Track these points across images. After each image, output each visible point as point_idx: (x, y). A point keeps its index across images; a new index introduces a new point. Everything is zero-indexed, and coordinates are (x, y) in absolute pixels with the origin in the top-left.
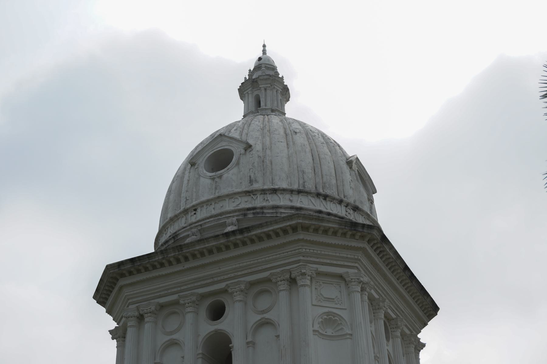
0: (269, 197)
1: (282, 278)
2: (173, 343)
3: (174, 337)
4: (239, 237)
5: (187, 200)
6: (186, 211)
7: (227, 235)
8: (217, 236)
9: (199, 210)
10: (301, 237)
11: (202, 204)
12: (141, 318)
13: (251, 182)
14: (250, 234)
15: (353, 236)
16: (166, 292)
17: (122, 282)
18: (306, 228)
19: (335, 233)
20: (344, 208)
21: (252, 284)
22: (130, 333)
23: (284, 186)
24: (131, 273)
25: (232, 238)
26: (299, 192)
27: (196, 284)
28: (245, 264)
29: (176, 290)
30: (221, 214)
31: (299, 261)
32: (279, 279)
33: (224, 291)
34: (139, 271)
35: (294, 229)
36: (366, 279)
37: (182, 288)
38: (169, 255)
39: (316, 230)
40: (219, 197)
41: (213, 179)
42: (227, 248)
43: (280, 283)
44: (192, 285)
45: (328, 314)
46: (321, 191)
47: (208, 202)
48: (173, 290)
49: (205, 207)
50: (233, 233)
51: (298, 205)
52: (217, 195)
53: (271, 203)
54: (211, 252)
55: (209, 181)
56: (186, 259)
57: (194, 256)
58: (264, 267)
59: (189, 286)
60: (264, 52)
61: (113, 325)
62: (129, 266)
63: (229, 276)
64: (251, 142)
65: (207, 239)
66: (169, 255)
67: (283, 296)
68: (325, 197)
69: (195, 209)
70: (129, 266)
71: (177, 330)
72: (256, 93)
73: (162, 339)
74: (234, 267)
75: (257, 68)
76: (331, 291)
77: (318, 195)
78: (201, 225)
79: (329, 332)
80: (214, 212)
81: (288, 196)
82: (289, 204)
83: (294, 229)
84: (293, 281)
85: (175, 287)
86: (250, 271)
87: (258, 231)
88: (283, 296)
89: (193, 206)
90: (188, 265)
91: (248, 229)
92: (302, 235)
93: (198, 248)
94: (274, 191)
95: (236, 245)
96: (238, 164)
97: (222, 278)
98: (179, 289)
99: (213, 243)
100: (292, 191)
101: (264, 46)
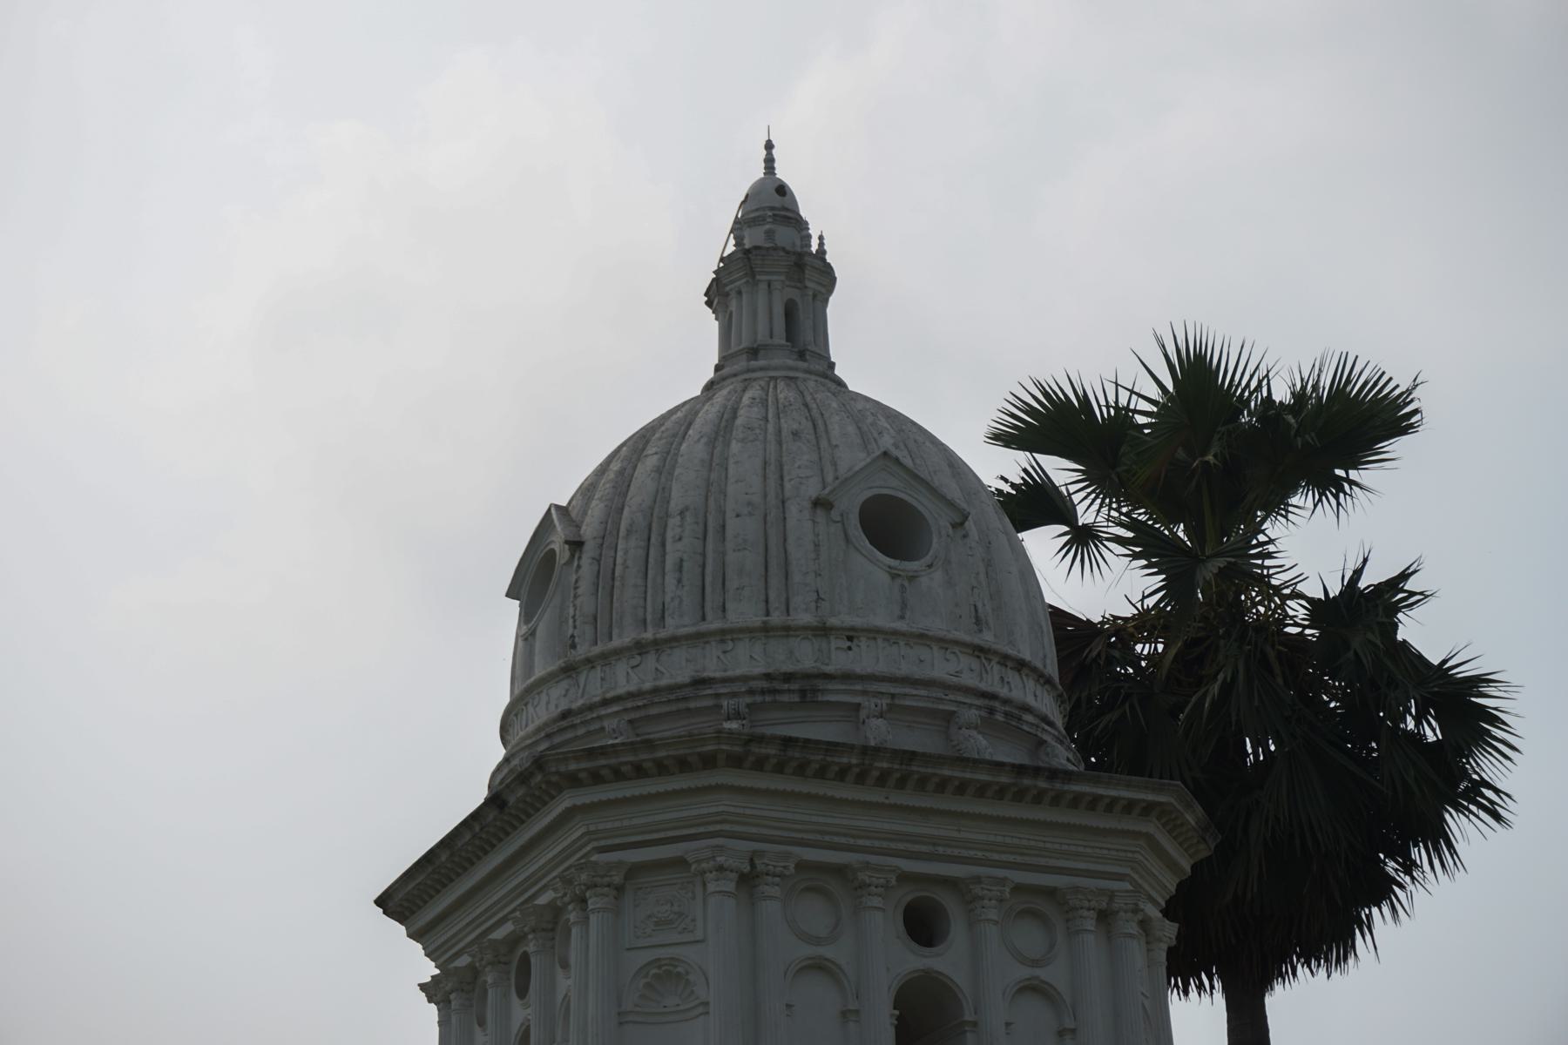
1: (1093, 904)
4: (1042, 784)
5: (819, 599)
6: (823, 631)
8: (1000, 765)
9: (863, 643)
11: (874, 633)
12: (748, 880)
13: (978, 621)
14: (1066, 787)
16: (819, 837)
24: (759, 765)
25: (1027, 782)
27: (893, 845)
28: (1016, 841)
29: (843, 840)
32: (1086, 904)
37: (860, 842)
38: (877, 764)
40: (922, 636)
41: (894, 577)
42: (1001, 793)
43: (1086, 913)
44: (885, 844)
47: (892, 636)
48: (836, 839)
49: (880, 641)
57: (922, 784)
58: (1053, 862)
59: (877, 843)
60: (769, 162)
62: (773, 752)
63: (972, 853)
66: (877, 764)
69: (851, 635)
74: (992, 838)
78: (893, 696)
80: (905, 669)
85: (845, 835)
86: (1019, 859)
89: (853, 629)
92: (1151, 827)
93: (947, 772)
95: (1019, 796)
97: (956, 852)
98: (852, 841)
101: (769, 146)
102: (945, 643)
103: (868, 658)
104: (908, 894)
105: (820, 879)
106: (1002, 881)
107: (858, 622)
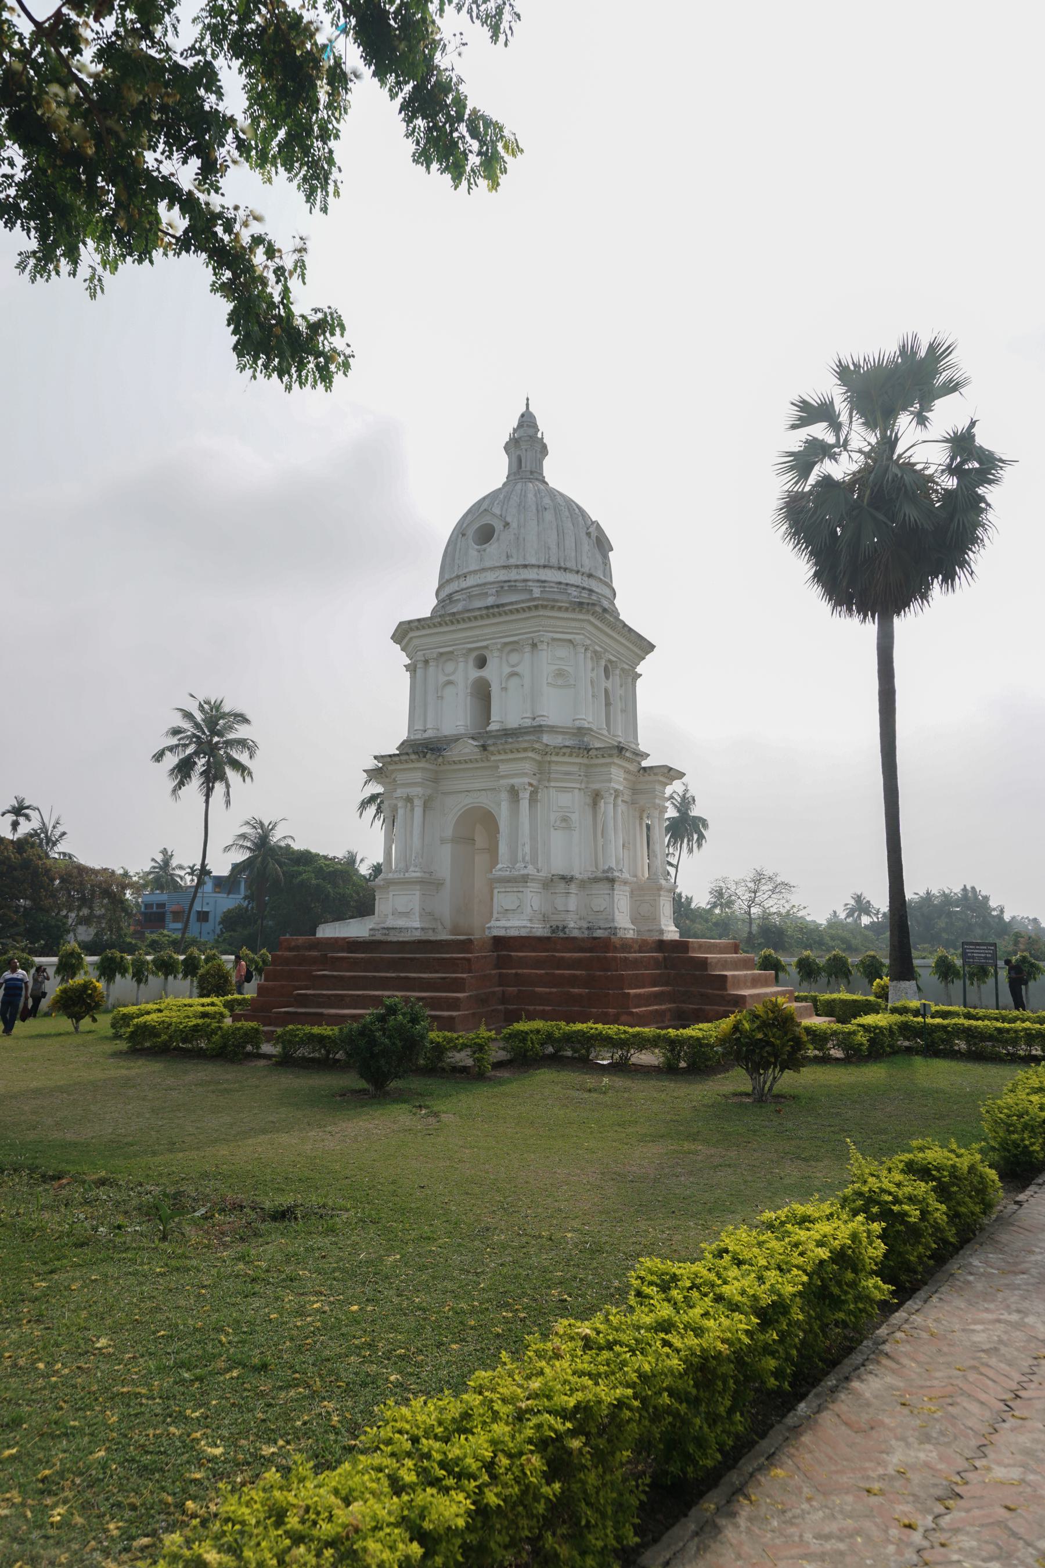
0: (521, 571)
2: (450, 683)
3: (451, 678)
4: (496, 610)
6: (458, 577)
7: (487, 608)
8: (480, 608)
10: (541, 613)
11: (470, 573)
12: (426, 662)
13: (508, 557)
15: (580, 611)
17: (411, 634)
18: (544, 607)
19: (567, 609)
20: (580, 576)
21: (506, 644)
22: (419, 672)
23: (534, 561)
24: (418, 629)
26: (545, 567)
30: (485, 584)
31: (539, 631)
33: (486, 647)
34: (424, 628)
35: (536, 607)
36: (588, 642)
39: (553, 607)
42: (488, 616)
45: (559, 670)
46: (562, 565)
47: (475, 572)
50: (492, 607)
51: (543, 578)
52: (482, 566)
53: (523, 577)
54: (476, 618)
55: (476, 553)
56: (458, 622)
61: (408, 661)
64: (509, 519)
65: (473, 610)
67: (527, 656)
68: (565, 569)
70: (416, 624)
71: (453, 673)
72: (518, 453)
73: (443, 679)
75: (521, 425)
76: (562, 652)
77: (560, 568)
79: (560, 682)
81: (536, 570)
82: (536, 577)
83: (536, 607)
84: (534, 645)
87: (510, 607)
88: (527, 656)
90: (460, 626)
91: (503, 605)
92: (541, 612)
94: (525, 566)
95: (494, 615)
96: (498, 539)
99: (477, 613)
100: (539, 566)
102: (492, 569)
103: (471, 581)
104: (474, 654)
105: (446, 657)
106: (496, 644)
107: (465, 571)
